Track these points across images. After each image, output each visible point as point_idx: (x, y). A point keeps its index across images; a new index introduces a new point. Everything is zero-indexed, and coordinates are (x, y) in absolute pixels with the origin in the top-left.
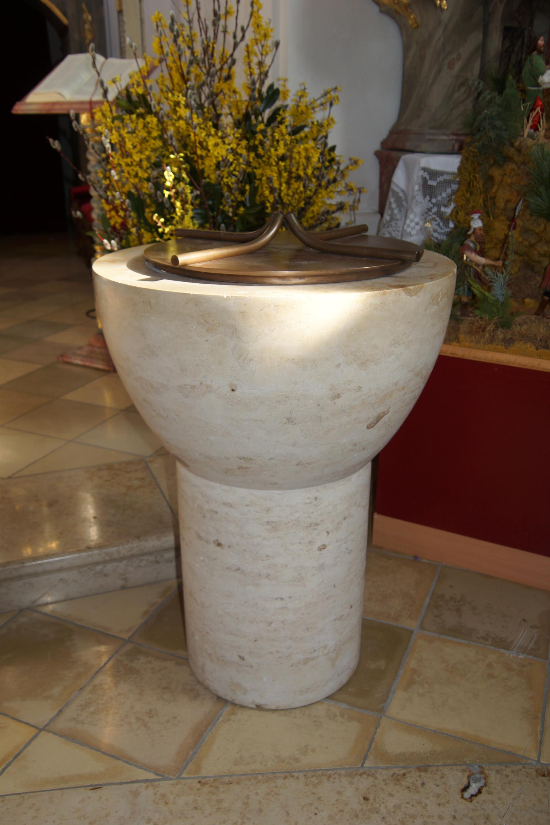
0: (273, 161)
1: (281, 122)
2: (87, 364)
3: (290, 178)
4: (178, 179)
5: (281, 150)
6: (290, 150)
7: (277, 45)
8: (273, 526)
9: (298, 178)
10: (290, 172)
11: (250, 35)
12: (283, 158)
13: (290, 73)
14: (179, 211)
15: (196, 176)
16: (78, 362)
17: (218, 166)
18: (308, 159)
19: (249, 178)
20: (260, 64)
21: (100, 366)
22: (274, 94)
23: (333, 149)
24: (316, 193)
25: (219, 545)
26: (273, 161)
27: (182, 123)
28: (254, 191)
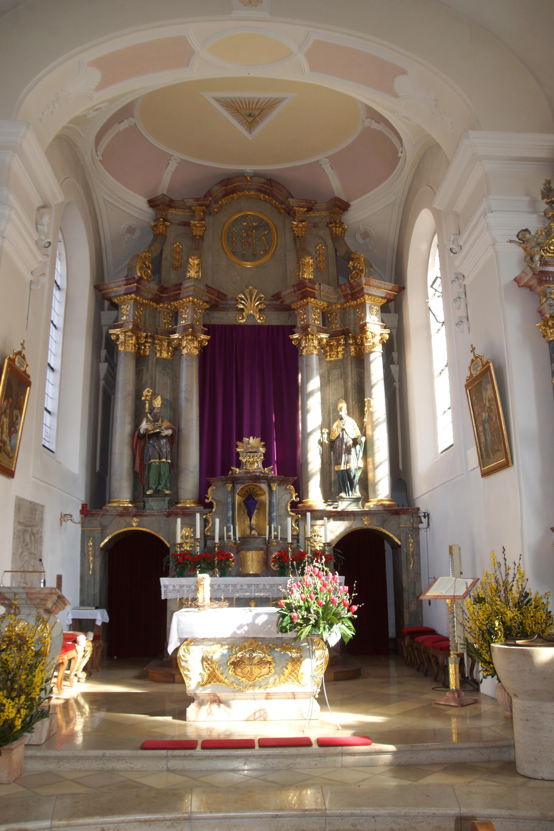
0: (529, 617)
1: (530, 605)
2: (447, 704)
3: (535, 623)
4: (499, 624)
5: (532, 614)
6: (535, 614)
7: (527, 580)
8: (542, 713)
9: (538, 623)
10: (535, 621)
11: (517, 576)
12: (532, 617)
13: (533, 588)
14: (500, 635)
15: (504, 623)
16: (443, 703)
17: (511, 620)
18: (541, 617)
19: (521, 623)
20: (522, 585)
21: (454, 704)
22: (527, 594)
23: (550, 612)
24: (545, 628)
25: (527, 720)
26: (529, 617)
27: (498, 606)
28: (524, 628)
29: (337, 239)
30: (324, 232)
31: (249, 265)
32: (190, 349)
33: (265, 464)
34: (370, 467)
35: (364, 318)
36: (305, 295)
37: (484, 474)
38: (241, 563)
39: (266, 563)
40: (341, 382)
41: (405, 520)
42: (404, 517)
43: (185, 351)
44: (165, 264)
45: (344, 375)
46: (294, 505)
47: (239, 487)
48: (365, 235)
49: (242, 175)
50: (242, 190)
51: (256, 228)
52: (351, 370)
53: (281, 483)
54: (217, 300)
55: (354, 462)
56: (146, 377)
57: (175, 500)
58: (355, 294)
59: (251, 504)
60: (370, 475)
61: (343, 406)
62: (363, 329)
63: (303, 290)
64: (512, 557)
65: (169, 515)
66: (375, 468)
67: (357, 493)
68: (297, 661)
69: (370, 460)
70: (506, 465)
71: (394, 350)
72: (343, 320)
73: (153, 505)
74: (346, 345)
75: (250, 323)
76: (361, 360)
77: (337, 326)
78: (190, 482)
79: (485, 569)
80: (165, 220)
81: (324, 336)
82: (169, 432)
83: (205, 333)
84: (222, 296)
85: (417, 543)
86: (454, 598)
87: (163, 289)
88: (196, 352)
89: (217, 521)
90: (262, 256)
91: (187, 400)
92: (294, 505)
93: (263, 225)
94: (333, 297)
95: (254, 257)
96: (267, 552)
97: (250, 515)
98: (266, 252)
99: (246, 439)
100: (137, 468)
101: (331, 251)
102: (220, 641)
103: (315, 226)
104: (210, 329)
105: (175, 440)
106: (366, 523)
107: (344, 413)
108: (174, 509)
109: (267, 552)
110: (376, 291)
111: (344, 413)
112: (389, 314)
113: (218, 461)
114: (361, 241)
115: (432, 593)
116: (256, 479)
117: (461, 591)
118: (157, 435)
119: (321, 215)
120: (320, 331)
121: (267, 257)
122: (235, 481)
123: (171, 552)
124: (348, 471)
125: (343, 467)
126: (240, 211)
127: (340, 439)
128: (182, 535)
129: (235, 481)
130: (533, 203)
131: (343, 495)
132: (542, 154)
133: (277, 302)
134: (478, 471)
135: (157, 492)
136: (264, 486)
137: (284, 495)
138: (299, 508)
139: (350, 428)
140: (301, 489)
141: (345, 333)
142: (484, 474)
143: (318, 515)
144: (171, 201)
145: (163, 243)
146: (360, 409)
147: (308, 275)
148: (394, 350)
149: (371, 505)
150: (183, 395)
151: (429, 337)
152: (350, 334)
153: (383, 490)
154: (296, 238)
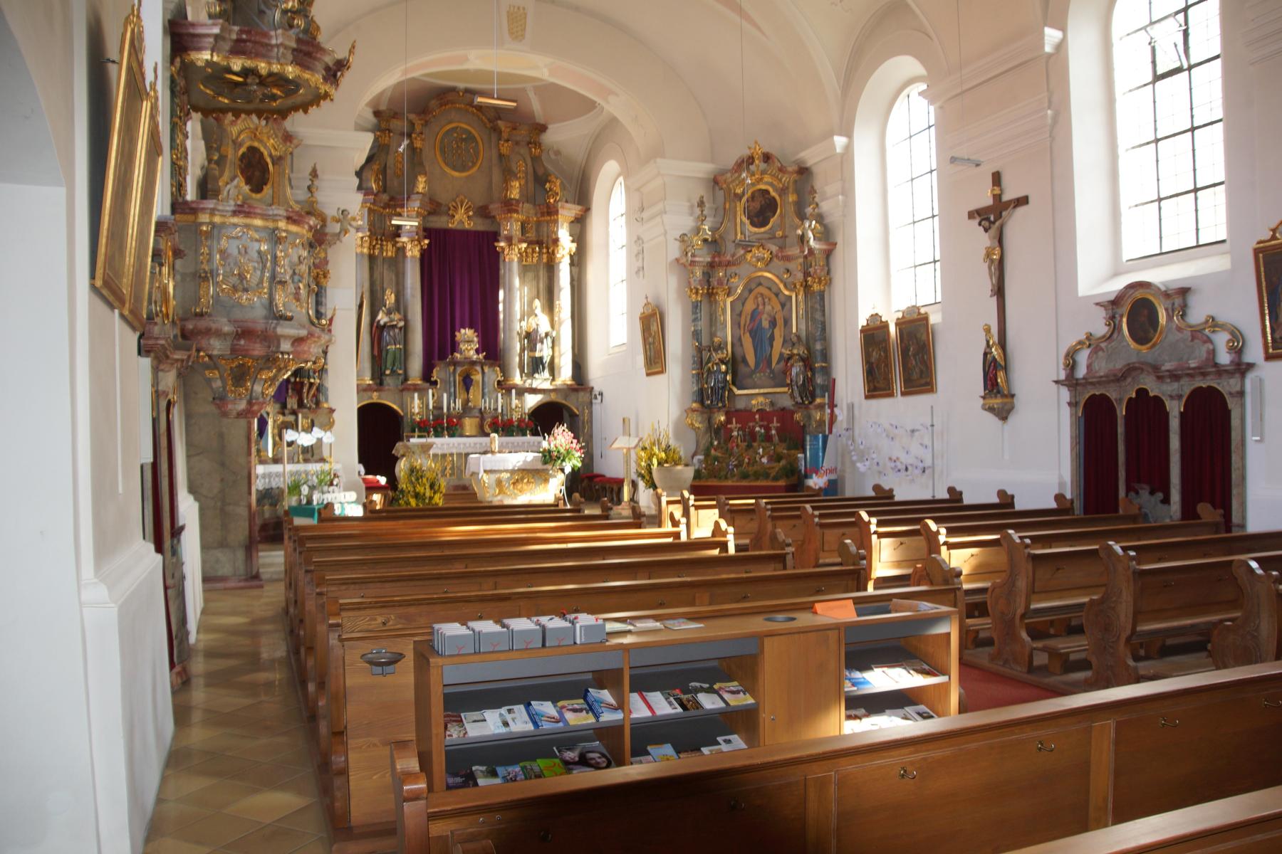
13: (672, 443)
29: (536, 160)
30: (524, 151)
31: (456, 174)
32: (413, 252)
33: (477, 351)
34: (556, 354)
35: (556, 233)
36: (511, 211)
37: (648, 375)
38: (462, 426)
39: (481, 427)
40: (534, 283)
41: (582, 396)
42: (581, 394)
43: (409, 254)
44: (388, 171)
45: (537, 278)
46: (499, 382)
47: (459, 370)
48: (558, 153)
49: (453, 90)
50: (453, 103)
51: (463, 140)
52: (543, 274)
53: (491, 366)
54: (434, 207)
55: (544, 351)
56: (377, 275)
57: (406, 379)
58: (551, 212)
59: (467, 382)
60: (556, 360)
61: (537, 303)
62: (556, 241)
63: (510, 207)
64: (663, 426)
65: (402, 391)
66: (560, 356)
67: (546, 374)
68: (546, 481)
69: (556, 349)
70: (661, 372)
71: (578, 261)
72: (537, 231)
73: (389, 381)
74: (540, 253)
75: (460, 227)
76: (551, 267)
77: (531, 235)
78: (416, 365)
79: (646, 433)
80: (390, 131)
81: (524, 245)
82: (402, 324)
83: (426, 237)
84: (439, 205)
85: (591, 413)
86: (629, 449)
87: (392, 199)
88: (417, 253)
89: (445, 395)
90: (470, 168)
91: (413, 296)
92: (499, 382)
93: (471, 138)
94: (532, 212)
95: (463, 168)
96: (482, 419)
97: (468, 391)
98: (474, 164)
99: (463, 331)
100: (376, 353)
101: (530, 170)
102: (506, 471)
103: (517, 143)
104: (428, 232)
105: (405, 329)
106: (553, 397)
107: (538, 311)
108: (406, 387)
109: (482, 419)
110: (567, 212)
111: (538, 311)
112: (640, 359)
113: (440, 347)
114: (553, 157)
115: (615, 446)
116: (473, 363)
117: (633, 445)
118: (394, 327)
119: (523, 133)
120: (521, 241)
121: (476, 168)
122: (455, 363)
123: (407, 421)
124: (541, 358)
125: (537, 354)
126: (450, 122)
127: (536, 331)
128: (416, 406)
129: (455, 363)
130: (692, 207)
131: (536, 375)
132: (701, 175)
133: (483, 212)
134: (644, 371)
135: (393, 372)
136: (479, 368)
137: (493, 375)
138: (505, 387)
139: (541, 323)
140: (505, 371)
141: (540, 243)
142: (648, 375)
143: (521, 392)
144: (396, 114)
145: (387, 153)
146: (550, 306)
147: (515, 194)
148: (578, 261)
149: (559, 382)
150: (409, 291)
151: (607, 255)
152: (546, 244)
153: (566, 374)
154: (501, 156)
